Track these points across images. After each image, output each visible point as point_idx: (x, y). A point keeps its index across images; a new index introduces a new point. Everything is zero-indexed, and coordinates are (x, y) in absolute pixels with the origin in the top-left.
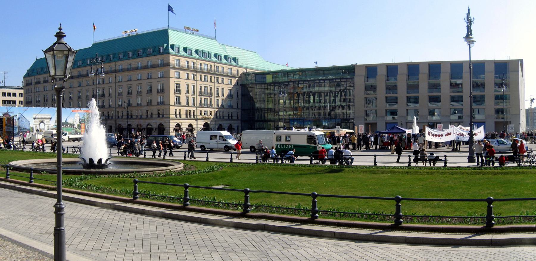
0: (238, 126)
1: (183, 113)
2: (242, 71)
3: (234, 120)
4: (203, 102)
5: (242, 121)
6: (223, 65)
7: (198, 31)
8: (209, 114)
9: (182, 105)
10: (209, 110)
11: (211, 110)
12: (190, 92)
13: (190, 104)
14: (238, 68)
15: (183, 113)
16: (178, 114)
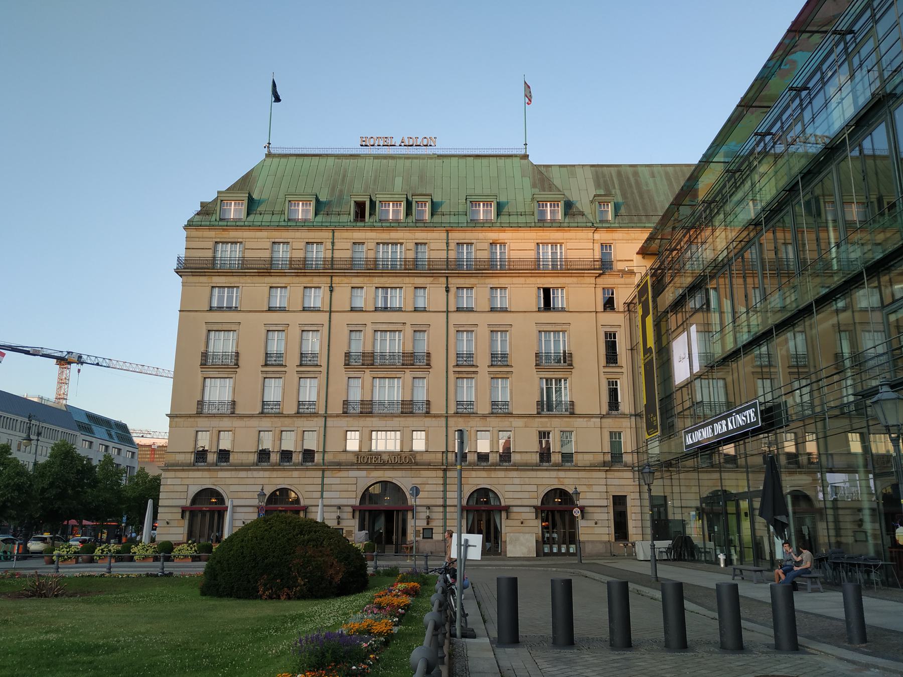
0: (619, 502)
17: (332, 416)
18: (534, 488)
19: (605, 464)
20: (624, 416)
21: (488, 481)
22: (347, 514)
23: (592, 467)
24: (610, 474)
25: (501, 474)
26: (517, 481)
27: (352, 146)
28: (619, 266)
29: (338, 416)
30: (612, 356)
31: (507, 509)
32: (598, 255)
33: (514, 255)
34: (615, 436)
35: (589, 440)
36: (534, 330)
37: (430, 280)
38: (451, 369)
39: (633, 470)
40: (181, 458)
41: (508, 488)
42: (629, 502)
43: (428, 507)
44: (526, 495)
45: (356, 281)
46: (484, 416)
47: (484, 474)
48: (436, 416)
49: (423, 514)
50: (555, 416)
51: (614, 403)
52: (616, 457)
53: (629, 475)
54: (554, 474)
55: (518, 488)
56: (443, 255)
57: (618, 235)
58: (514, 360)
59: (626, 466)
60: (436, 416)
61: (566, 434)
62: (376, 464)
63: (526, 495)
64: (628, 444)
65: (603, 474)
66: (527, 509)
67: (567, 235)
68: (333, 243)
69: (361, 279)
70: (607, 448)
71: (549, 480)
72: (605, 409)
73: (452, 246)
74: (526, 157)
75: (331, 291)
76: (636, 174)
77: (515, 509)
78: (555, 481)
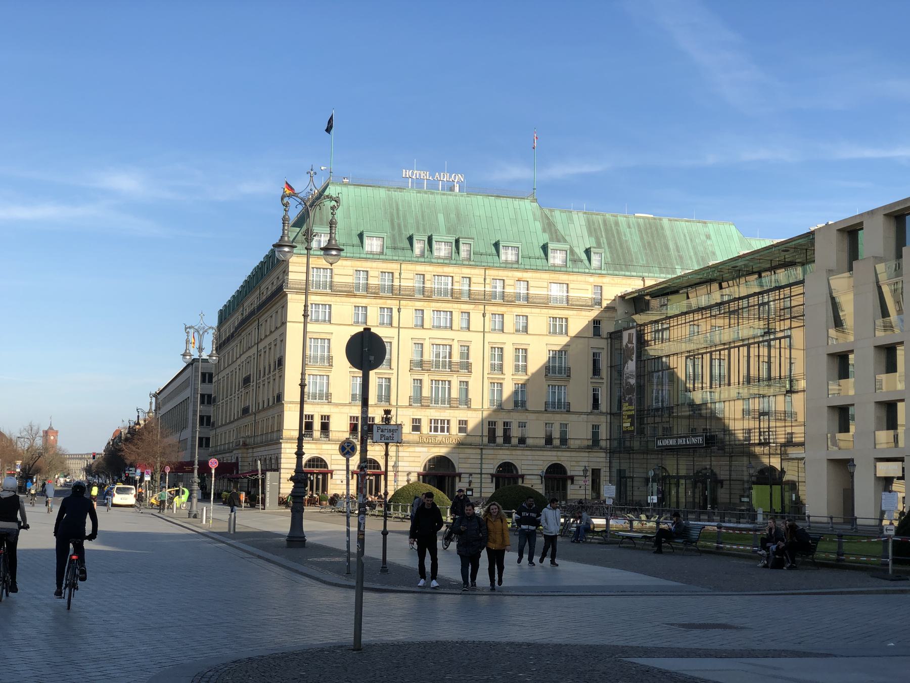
17: (401, 407)
18: (541, 463)
19: (588, 447)
20: (602, 413)
21: (511, 457)
23: (580, 449)
24: (592, 455)
25: (519, 452)
26: (530, 458)
29: (406, 407)
30: (596, 371)
31: (522, 476)
37: (472, 306)
38: (486, 376)
39: (606, 453)
41: (523, 462)
42: (602, 473)
43: (471, 474)
44: (535, 467)
46: (509, 411)
47: (507, 452)
48: (475, 410)
49: (465, 479)
50: (557, 413)
53: (603, 455)
54: (554, 453)
55: (530, 462)
57: (606, 280)
59: (601, 448)
60: (475, 410)
62: (436, 444)
63: (535, 467)
64: (603, 434)
65: (586, 454)
66: (536, 477)
68: (400, 274)
69: (422, 303)
70: (590, 436)
72: (589, 408)
75: (399, 312)
77: (528, 477)
78: (555, 458)
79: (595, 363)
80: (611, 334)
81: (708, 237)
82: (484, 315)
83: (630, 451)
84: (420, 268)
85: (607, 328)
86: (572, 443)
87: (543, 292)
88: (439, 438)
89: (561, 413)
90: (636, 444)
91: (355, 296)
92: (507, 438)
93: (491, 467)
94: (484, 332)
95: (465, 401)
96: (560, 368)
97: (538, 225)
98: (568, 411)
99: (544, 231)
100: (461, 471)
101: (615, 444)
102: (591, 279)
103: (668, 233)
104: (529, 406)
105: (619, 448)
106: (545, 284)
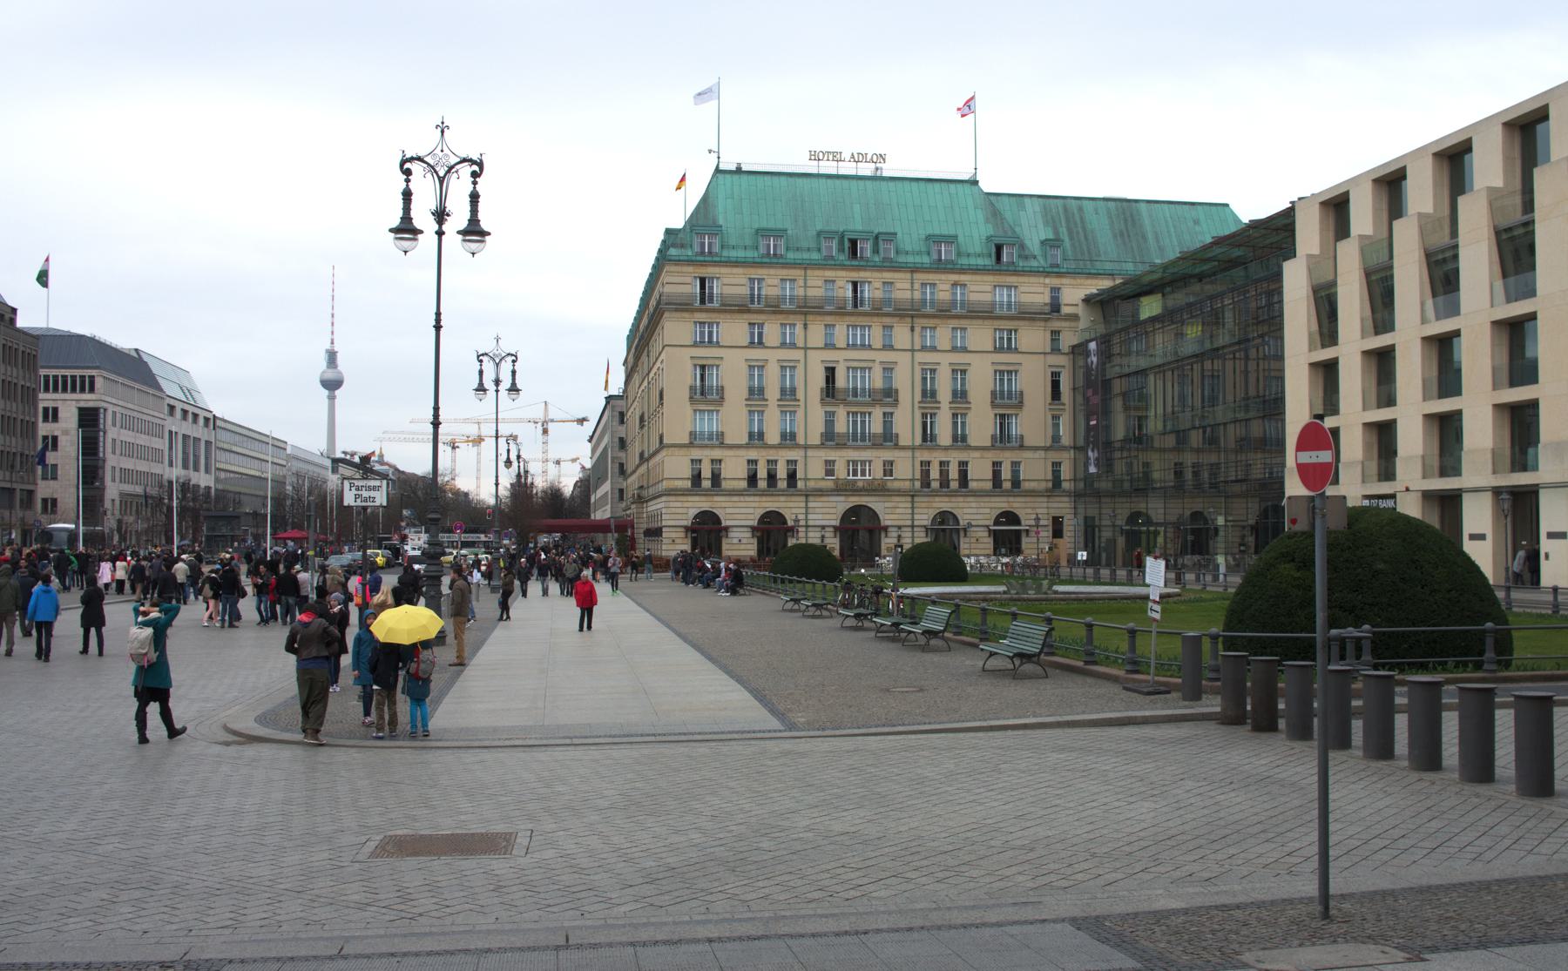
1: (734, 470)
2: (1074, 294)
3: (1032, 493)
4: (841, 426)
5: (1077, 496)
6: (963, 278)
7: (882, 157)
8: (879, 474)
9: (728, 441)
10: (877, 457)
11: (888, 455)
12: (773, 393)
13: (773, 437)
14: (1055, 282)
15: (734, 470)
16: (704, 481)
20: (1064, 448)
22: (829, 534)
27: (797, 160)
28: (1065, 310)
32: (1047, 300)
33: (974, 297)
34: (1056, 466)
35: (1035, 470)
36: (990, 370)
40: (679, 484)
43: (900, 527)
45: (829, 320)
46: (946, 448)
48: (904, 448)
49: (893, 533)
51: (1056, 438)
52: (1057, 481)
56: (908, 295)
57: (1064, 281)
58: (972, 396)
60: (904, 448)
61: (1015, 464)
64: (1066, 472)
67: (1021, 279)
70: (1050, 476)
71: (1002, 504)
73: (917, 286)
74: (975, 182)
76: (1081, 209)
79: (1056, 385)
80: (1074, 347)
81: (1196, 222)
82: (912, 329)
83: (1098, 495)
84: (829, 274)
85: (1068, 340)
86: (1026, 486)
87: (987, 298)
88: (860, 484)
89: (1013, 449)
90: (1104, 485)
91: (749, 311)
92: (945, 482)
93: (924, 517)
94: (913, 350)
95: (888, 438)
96: (1010, 392)
97: (981, 216)
98: (1022, 447)
99: (987, 221)
100: (888, 523)
101: (1081, 485)
102: (1047, 281)
103: (1147, 222)
104: (973, 441)
105: (1086, 491)
106: (989, 288)
